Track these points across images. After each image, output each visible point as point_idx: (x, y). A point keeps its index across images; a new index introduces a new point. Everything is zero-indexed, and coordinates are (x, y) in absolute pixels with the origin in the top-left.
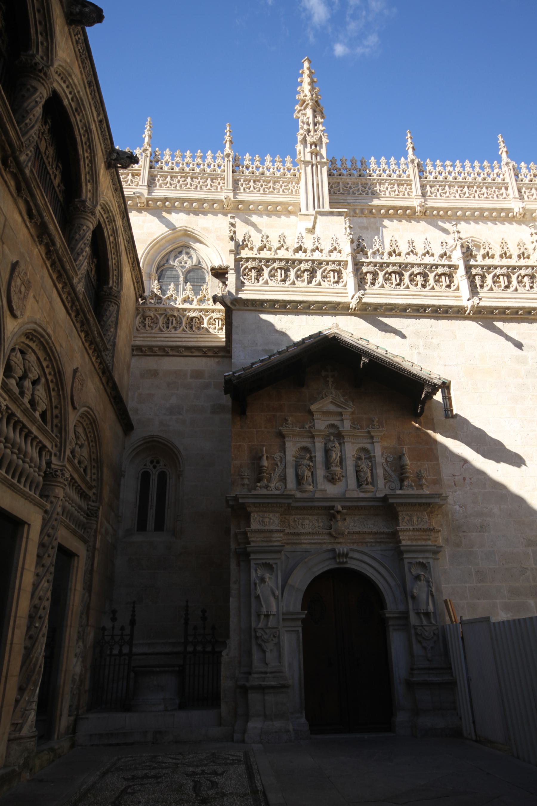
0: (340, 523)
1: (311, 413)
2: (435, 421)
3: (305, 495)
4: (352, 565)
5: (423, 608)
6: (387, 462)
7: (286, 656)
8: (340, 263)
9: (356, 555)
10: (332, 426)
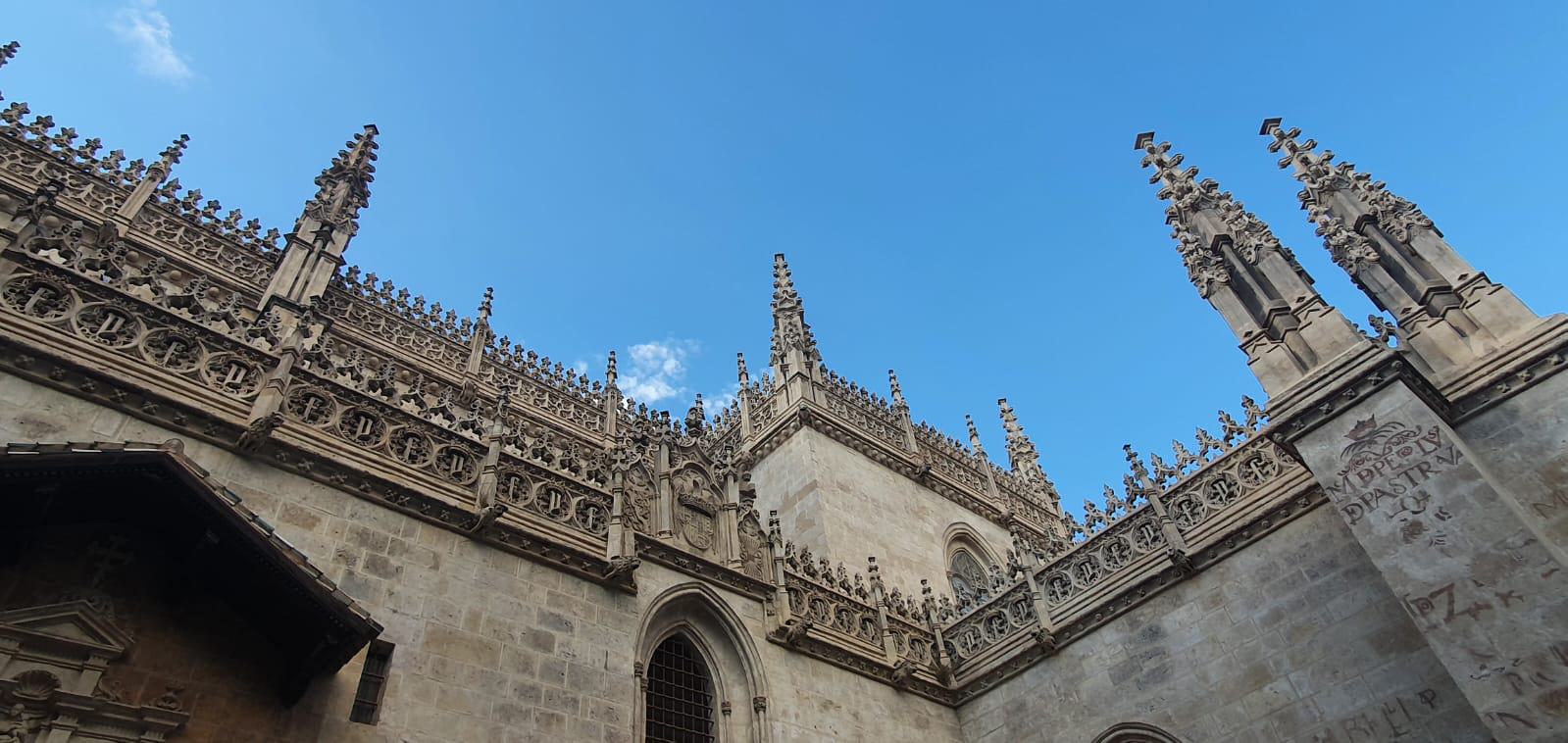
2: (325, 722)
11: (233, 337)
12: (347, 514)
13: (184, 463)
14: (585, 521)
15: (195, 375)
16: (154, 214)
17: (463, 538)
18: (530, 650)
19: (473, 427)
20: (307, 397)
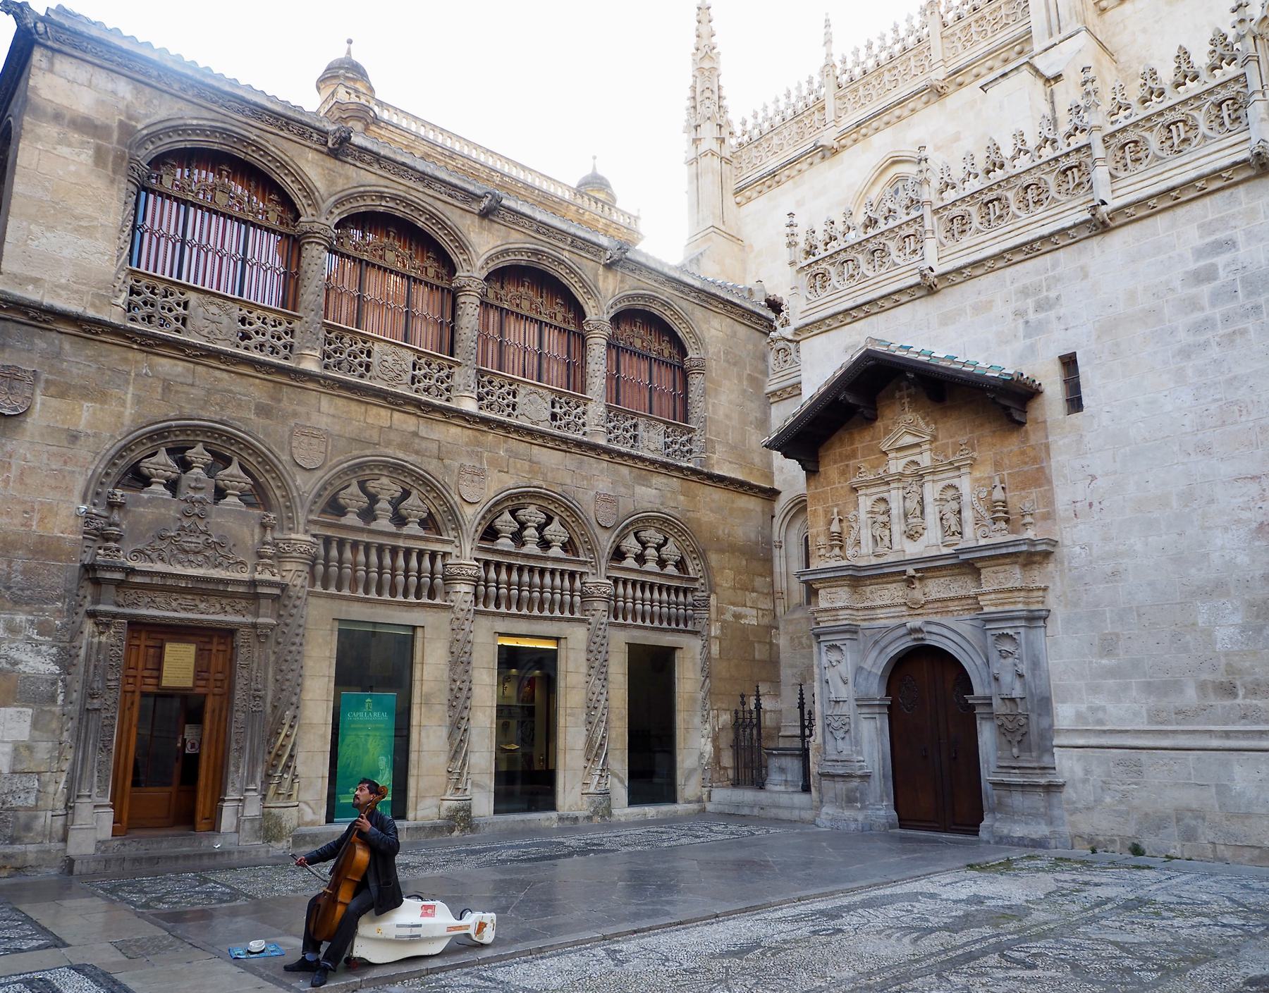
0: (916, 592)
1: (885, 453)
3: (881, 560)
4: (932, 641)
5: (1005, 691)
6: (980, 499)
7: (868, 744)
8: (914, 220)
9: (934, 629)
10: (913, 462)
11: (898, 222)
12: (1008, 283)
13: (878, 348)
14: (1222, 124)
15: (895, 264)
16: (953, 34)
17: (1099, 238)
18: (1194, 290)
19: (1076, 129)
20: (952, 220)
